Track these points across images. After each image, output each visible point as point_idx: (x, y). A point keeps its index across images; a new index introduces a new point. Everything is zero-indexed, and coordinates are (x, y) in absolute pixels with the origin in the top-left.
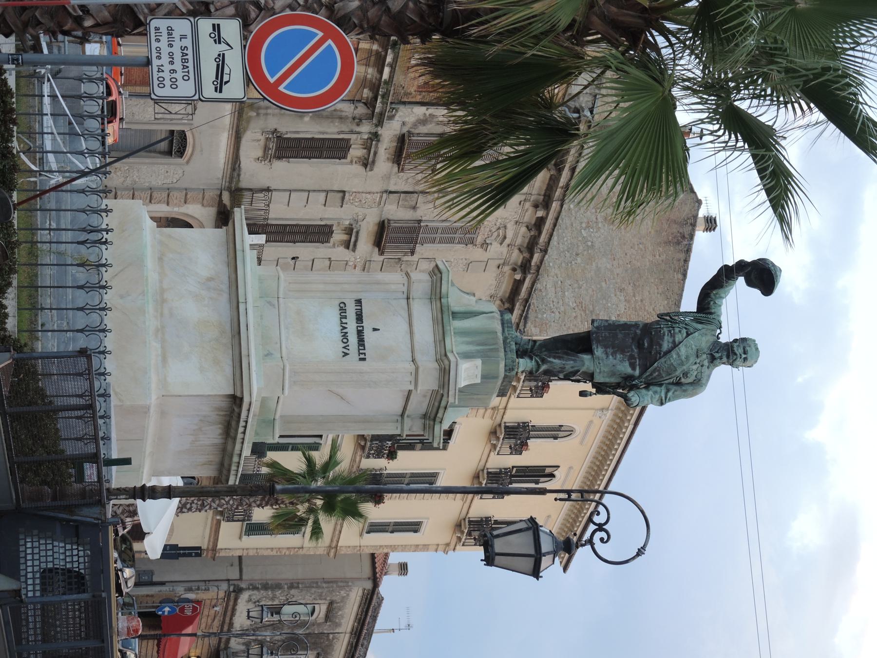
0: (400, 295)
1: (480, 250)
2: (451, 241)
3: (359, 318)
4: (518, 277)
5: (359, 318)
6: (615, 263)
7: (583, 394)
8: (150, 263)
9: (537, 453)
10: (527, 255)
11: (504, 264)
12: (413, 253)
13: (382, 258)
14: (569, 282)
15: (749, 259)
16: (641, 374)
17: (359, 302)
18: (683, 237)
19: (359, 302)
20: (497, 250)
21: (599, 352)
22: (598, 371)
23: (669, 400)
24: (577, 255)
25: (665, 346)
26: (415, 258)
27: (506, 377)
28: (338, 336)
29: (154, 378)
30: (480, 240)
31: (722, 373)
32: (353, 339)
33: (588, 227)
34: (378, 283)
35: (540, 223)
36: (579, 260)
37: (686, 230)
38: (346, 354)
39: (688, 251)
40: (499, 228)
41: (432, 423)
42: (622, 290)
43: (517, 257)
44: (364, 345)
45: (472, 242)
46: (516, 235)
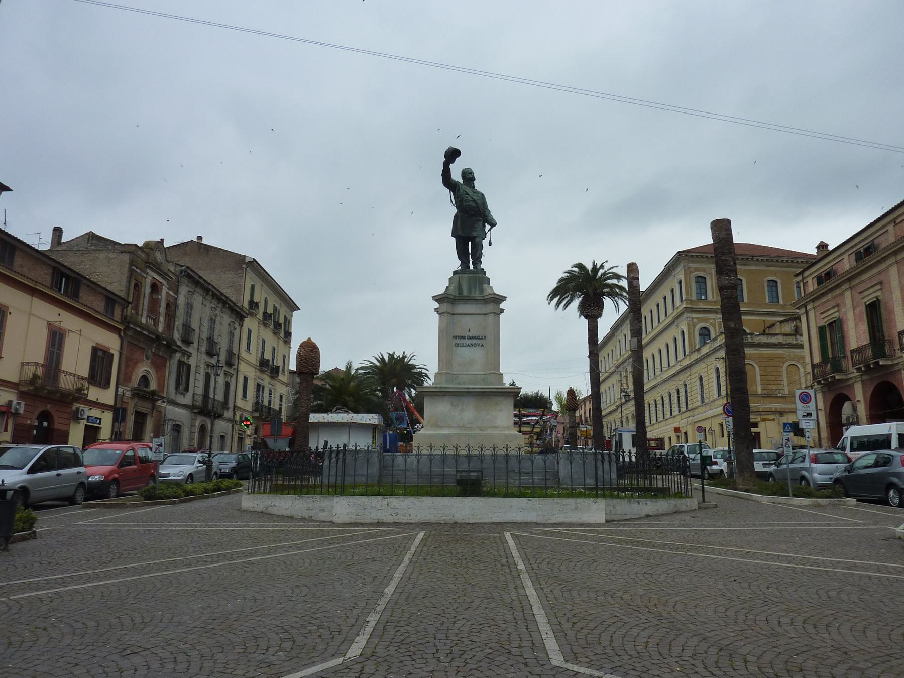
3: (463, 338)
5: (463, 338)
7: (490, 244)
8: (445, 432)
9: (270, 310)
17: (454, 337)
19: (454, 337)
21: (475, 234)
25: (474, 205)
28: (473, 348)
29: (507, 432)
31: (479, 185)
32: (474, 341)
35: (214, 295)
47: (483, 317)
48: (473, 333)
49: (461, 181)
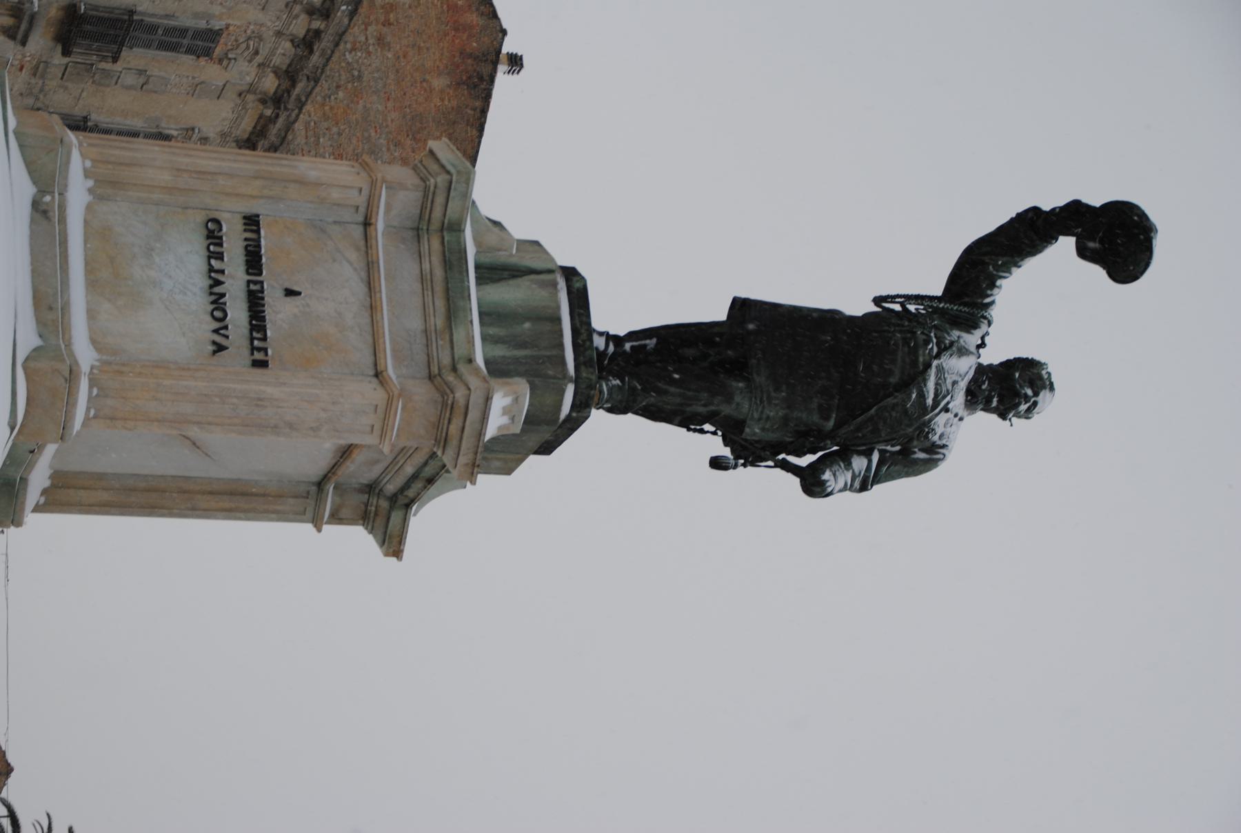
0: (348, 215)
1: (216, 67)
2: (173, 48)
3: (253, 261)
4: (268, 112)
5: (253, 261)
6: (390, 104)
7: (717, 463)
10: (286, 84)
11: (248, 91)
12: (115, 59)
13: (66, 60)
14: (326, 125)
15: (1096, 199)
16: (838, 425)
17: (252, 222)
18: (481, 79)
19: (252, 222)
20: (243, 72)
22: (756, 415)
23: (878, 482)
24: (338, 87)
26: (118, 67)
27: (569, 417)
28: (199, 302)
30: (218, 51)
32: (238, 313)
33: (353, 49)
34: (302, 182)
36: (341, 94)
37: (485, 70)
38: (219, 348)
39: (488, 96)
40: (249, 38)
41: (384, 504)
42: (398, 144)
43: (270, 83)
44: (262, 329)
45: (207, 53)
46: (273, 52)
47: (372, 372)
48: (278, 311)
49: (993, 356)
